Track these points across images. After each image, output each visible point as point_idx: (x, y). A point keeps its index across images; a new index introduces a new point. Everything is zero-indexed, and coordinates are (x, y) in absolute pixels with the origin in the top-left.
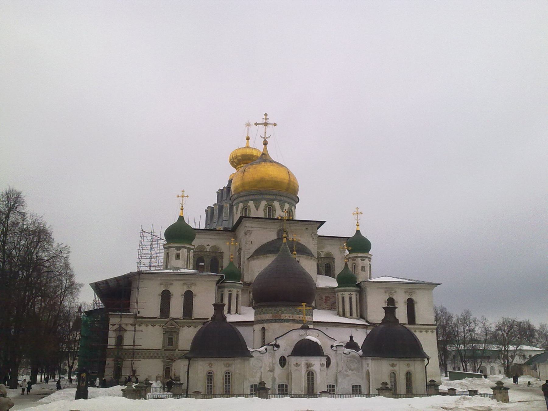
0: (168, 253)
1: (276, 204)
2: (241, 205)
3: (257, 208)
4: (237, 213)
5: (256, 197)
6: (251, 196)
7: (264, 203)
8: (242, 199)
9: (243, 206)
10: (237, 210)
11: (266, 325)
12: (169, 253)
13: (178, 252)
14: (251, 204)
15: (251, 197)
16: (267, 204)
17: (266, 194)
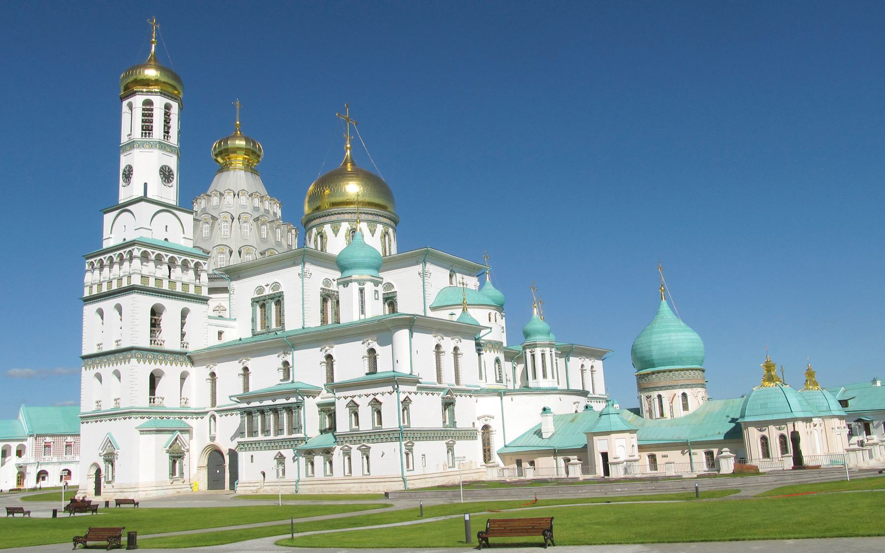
0: (362, 291)
1: (391, 231)
2: (345, 227)
3: (373, 233)
4: (336, 236)
5: (370, 217)
6: (364, 215)
7: (380, 228)
8: (347, 216)
9: (350, 228)
10: (336, 231)
11: (686, 391)
12: (364, 289)
13: (376, 288)
14: (363, 226)
15: (363, 216)
16: (383, 229)
17: (382, 216)
